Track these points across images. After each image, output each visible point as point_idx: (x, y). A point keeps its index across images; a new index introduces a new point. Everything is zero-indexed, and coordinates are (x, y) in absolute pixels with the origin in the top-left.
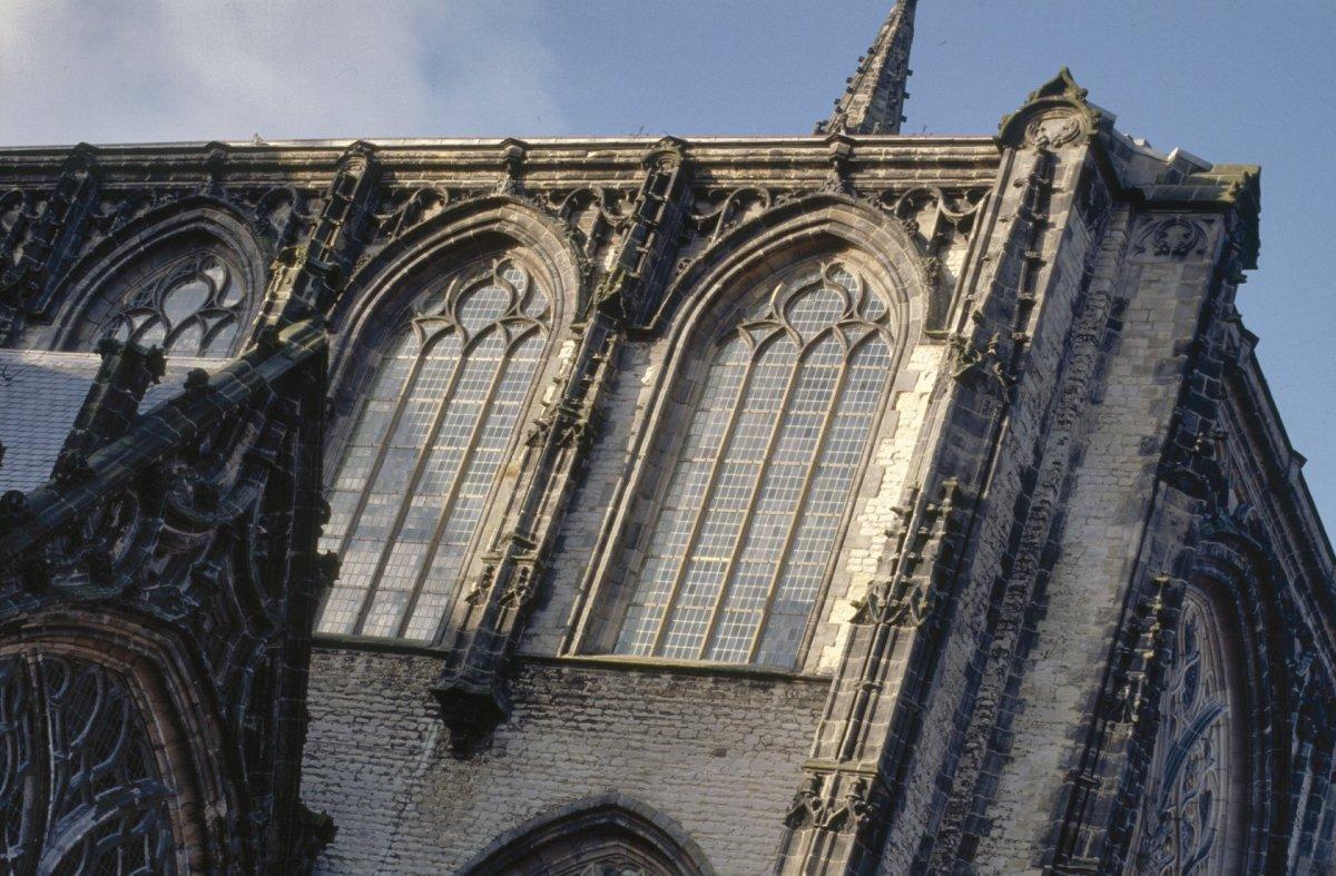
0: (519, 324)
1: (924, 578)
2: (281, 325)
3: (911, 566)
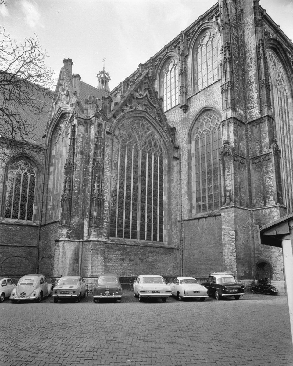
0: (175, 65)
1: (227, 55)
2: (142, 73)
3: (225, 54)
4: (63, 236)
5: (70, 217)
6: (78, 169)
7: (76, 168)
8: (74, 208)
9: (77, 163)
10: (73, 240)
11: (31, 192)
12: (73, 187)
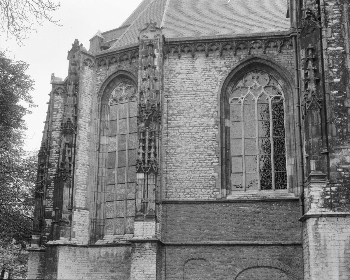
4: (313, 205)
5: (325, 151)
6: (335, 21)
7: (326, 21)
8: (336, 124)
9: (327, 8)
10: (343, 213)
11: (277, 131)
12: (326, 69)
